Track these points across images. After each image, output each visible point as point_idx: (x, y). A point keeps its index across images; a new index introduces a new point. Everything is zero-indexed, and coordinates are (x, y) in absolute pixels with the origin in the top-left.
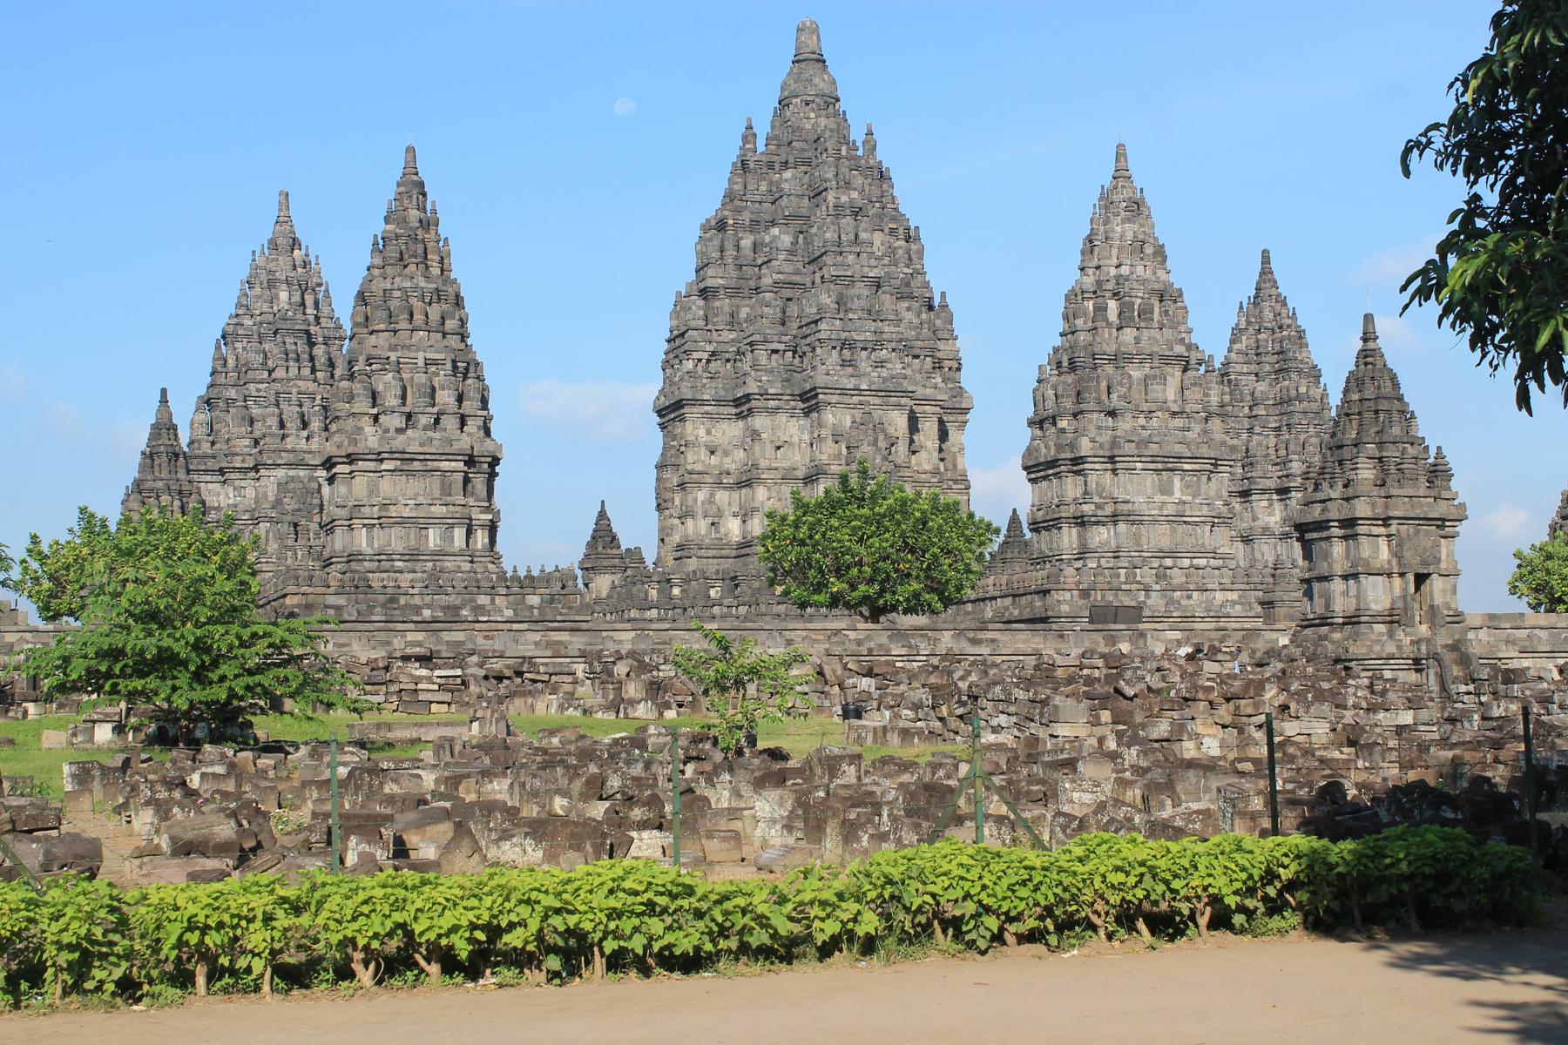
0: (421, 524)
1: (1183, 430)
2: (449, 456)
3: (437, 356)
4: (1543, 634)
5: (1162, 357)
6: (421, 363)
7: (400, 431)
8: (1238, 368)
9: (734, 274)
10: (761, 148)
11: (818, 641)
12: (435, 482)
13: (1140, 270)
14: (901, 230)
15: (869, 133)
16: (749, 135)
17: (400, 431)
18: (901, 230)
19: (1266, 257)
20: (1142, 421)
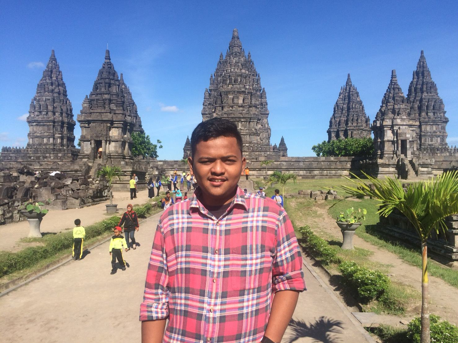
0: (42, 137)
1: (242, 110)
2: (49, 121)
3: (49, 98)
4: (284, 163)
5: (238, 92)
6: (44, 99)
7: (38, 116)
8: (340, 102)
9: (216, 86)
10: (224, 58)
11: (50, 165)
12: (46, 127)
13: (236, 70)
14: (255, 75)
15: (249, 53)
16: (221, 56)
17: (38, 116)
18: (255, 75)
19: (349, 75)
20: (231, 109)
